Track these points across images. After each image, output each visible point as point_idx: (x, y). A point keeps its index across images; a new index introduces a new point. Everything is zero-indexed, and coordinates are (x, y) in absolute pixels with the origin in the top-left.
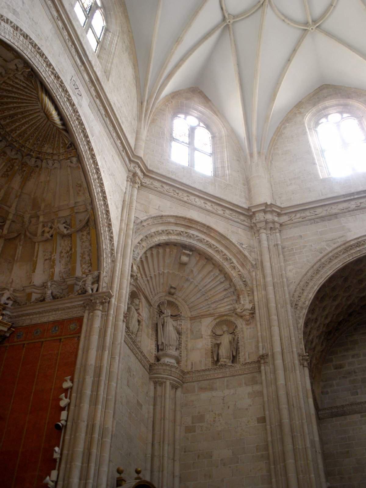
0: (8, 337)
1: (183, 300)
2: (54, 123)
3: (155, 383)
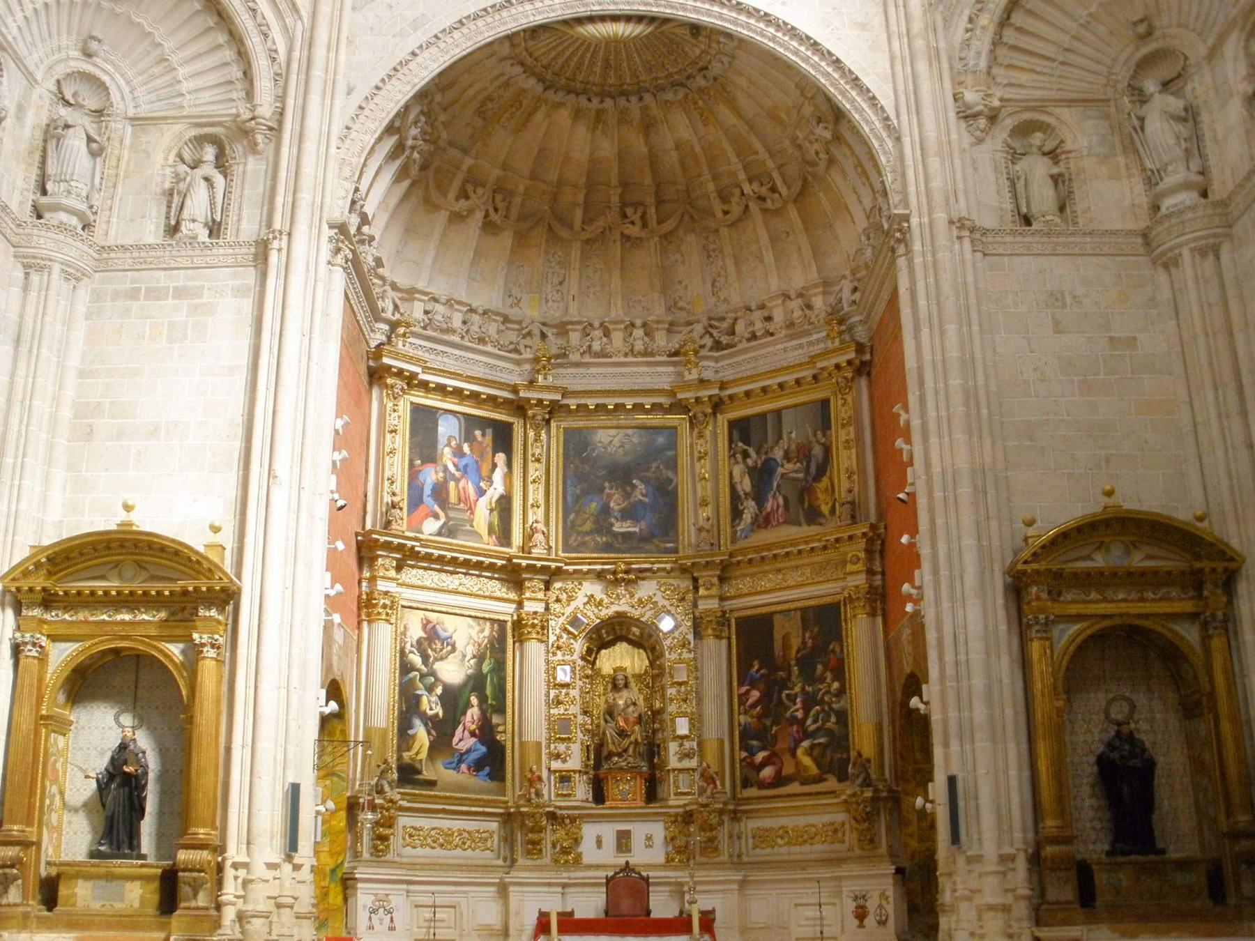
1: (1179, 26)
2: (635, 37)
3: (1166, 266)
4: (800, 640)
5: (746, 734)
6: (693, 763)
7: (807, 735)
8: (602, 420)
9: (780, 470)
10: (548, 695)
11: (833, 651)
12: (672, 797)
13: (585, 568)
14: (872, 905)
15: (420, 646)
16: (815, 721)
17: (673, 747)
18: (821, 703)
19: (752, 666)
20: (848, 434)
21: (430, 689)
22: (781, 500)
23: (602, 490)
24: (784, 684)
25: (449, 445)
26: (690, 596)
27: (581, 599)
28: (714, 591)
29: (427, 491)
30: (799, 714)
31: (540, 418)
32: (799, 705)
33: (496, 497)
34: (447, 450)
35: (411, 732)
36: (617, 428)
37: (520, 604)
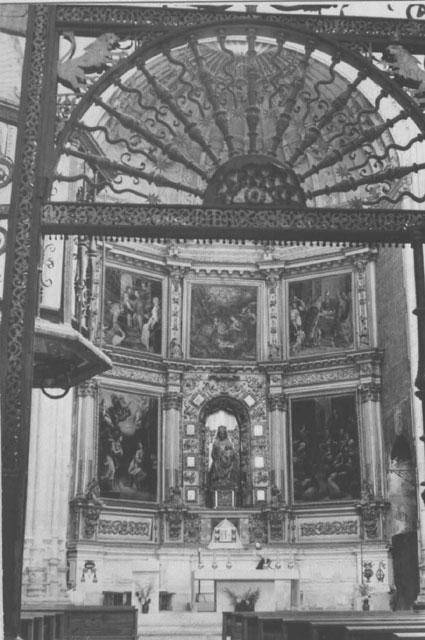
7: (333, 469)
9: (320, 314)
10: (181, 441)
14: (375, 569)
15: (111, 411)
20: (362, 296)
21: (116, 439)
22: (320, 332)
23: (213, 322)
25: (126, 292)
26: (264, 386)
28: (279, 383)
29: (115, 320)
33: (154, 323)
34: (126, 295)
35: (106, 464)
37: (166, 386)
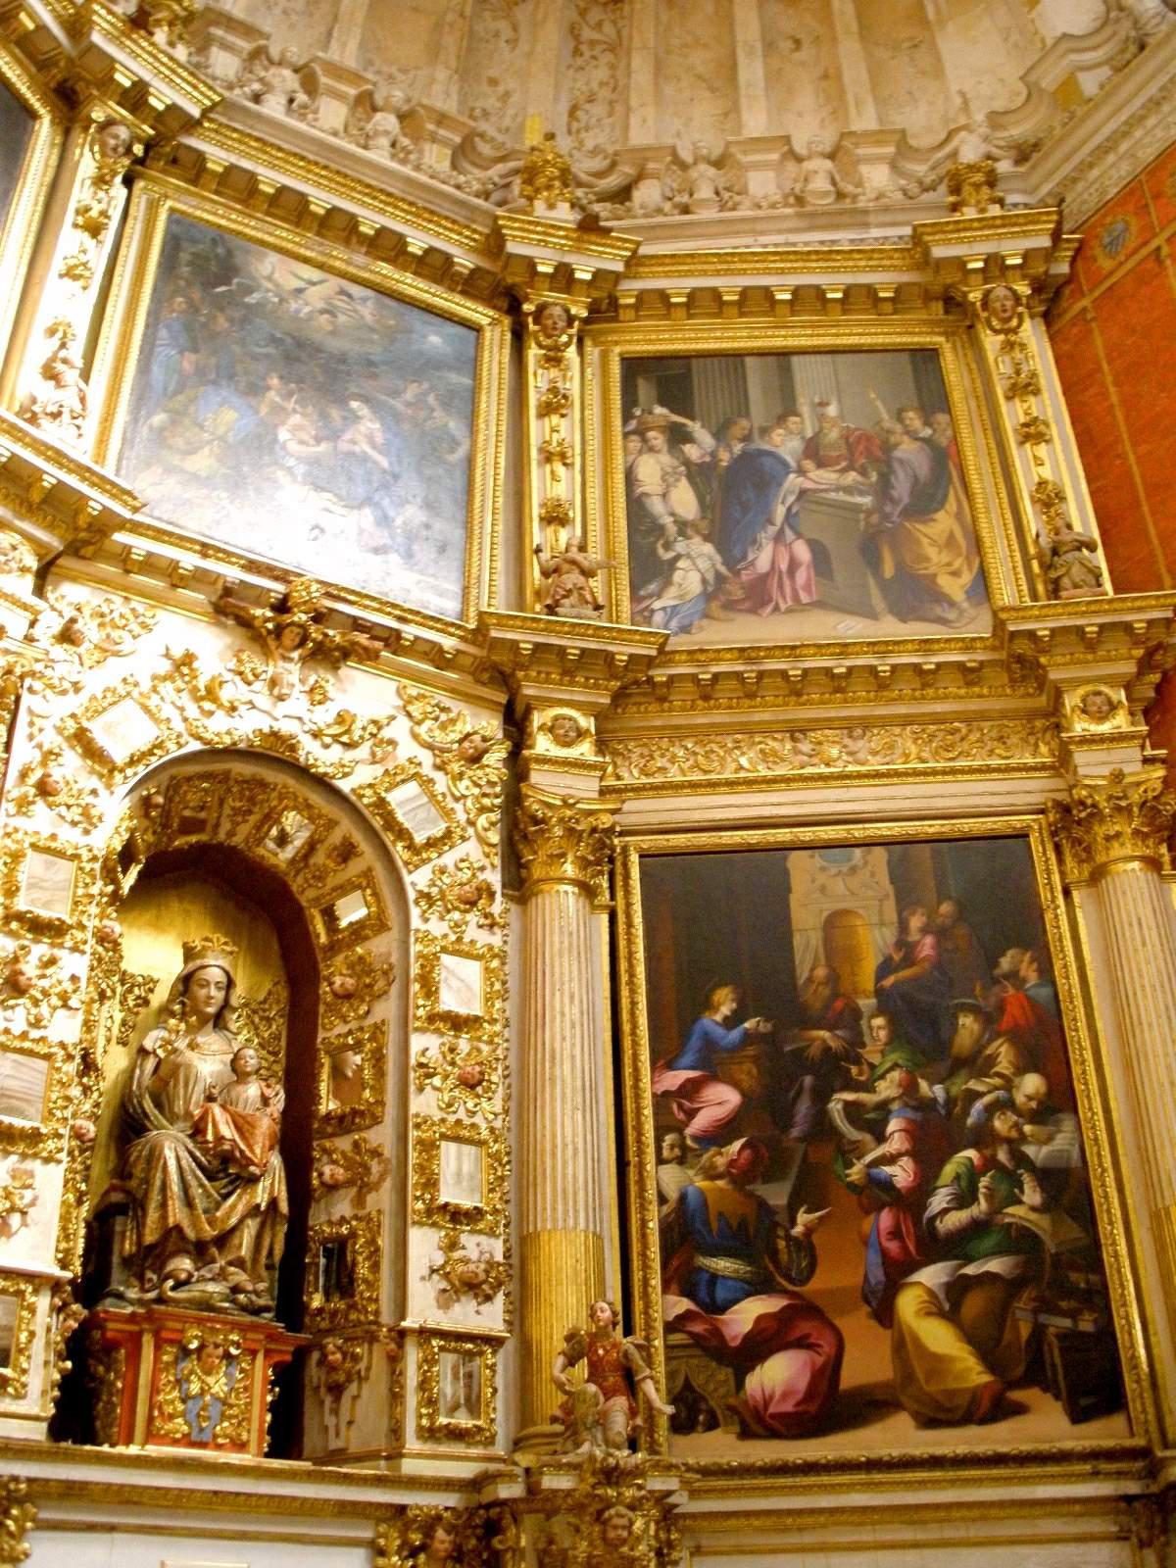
0: (1071, 279)
4: (890, 935)
5: (685, 1232)
6: (490, 1318)
7: (934, 1246)
8: (283, 234)
9: (793, 481)
11: (1013, 976)
12: (412, 1444)
13: (189, 560)
16: (964, 1198)
17: (424, 1245)
18: (982, 1137)
19: (708, 1005)
22: (802, 551)
24: (836, 1070)
26: (496, 757)
27: (145, 658)
30: (902, 1174)
31: (123, 133)
32: (896, 1143)
36: (321, 266)
